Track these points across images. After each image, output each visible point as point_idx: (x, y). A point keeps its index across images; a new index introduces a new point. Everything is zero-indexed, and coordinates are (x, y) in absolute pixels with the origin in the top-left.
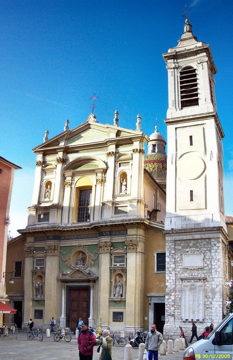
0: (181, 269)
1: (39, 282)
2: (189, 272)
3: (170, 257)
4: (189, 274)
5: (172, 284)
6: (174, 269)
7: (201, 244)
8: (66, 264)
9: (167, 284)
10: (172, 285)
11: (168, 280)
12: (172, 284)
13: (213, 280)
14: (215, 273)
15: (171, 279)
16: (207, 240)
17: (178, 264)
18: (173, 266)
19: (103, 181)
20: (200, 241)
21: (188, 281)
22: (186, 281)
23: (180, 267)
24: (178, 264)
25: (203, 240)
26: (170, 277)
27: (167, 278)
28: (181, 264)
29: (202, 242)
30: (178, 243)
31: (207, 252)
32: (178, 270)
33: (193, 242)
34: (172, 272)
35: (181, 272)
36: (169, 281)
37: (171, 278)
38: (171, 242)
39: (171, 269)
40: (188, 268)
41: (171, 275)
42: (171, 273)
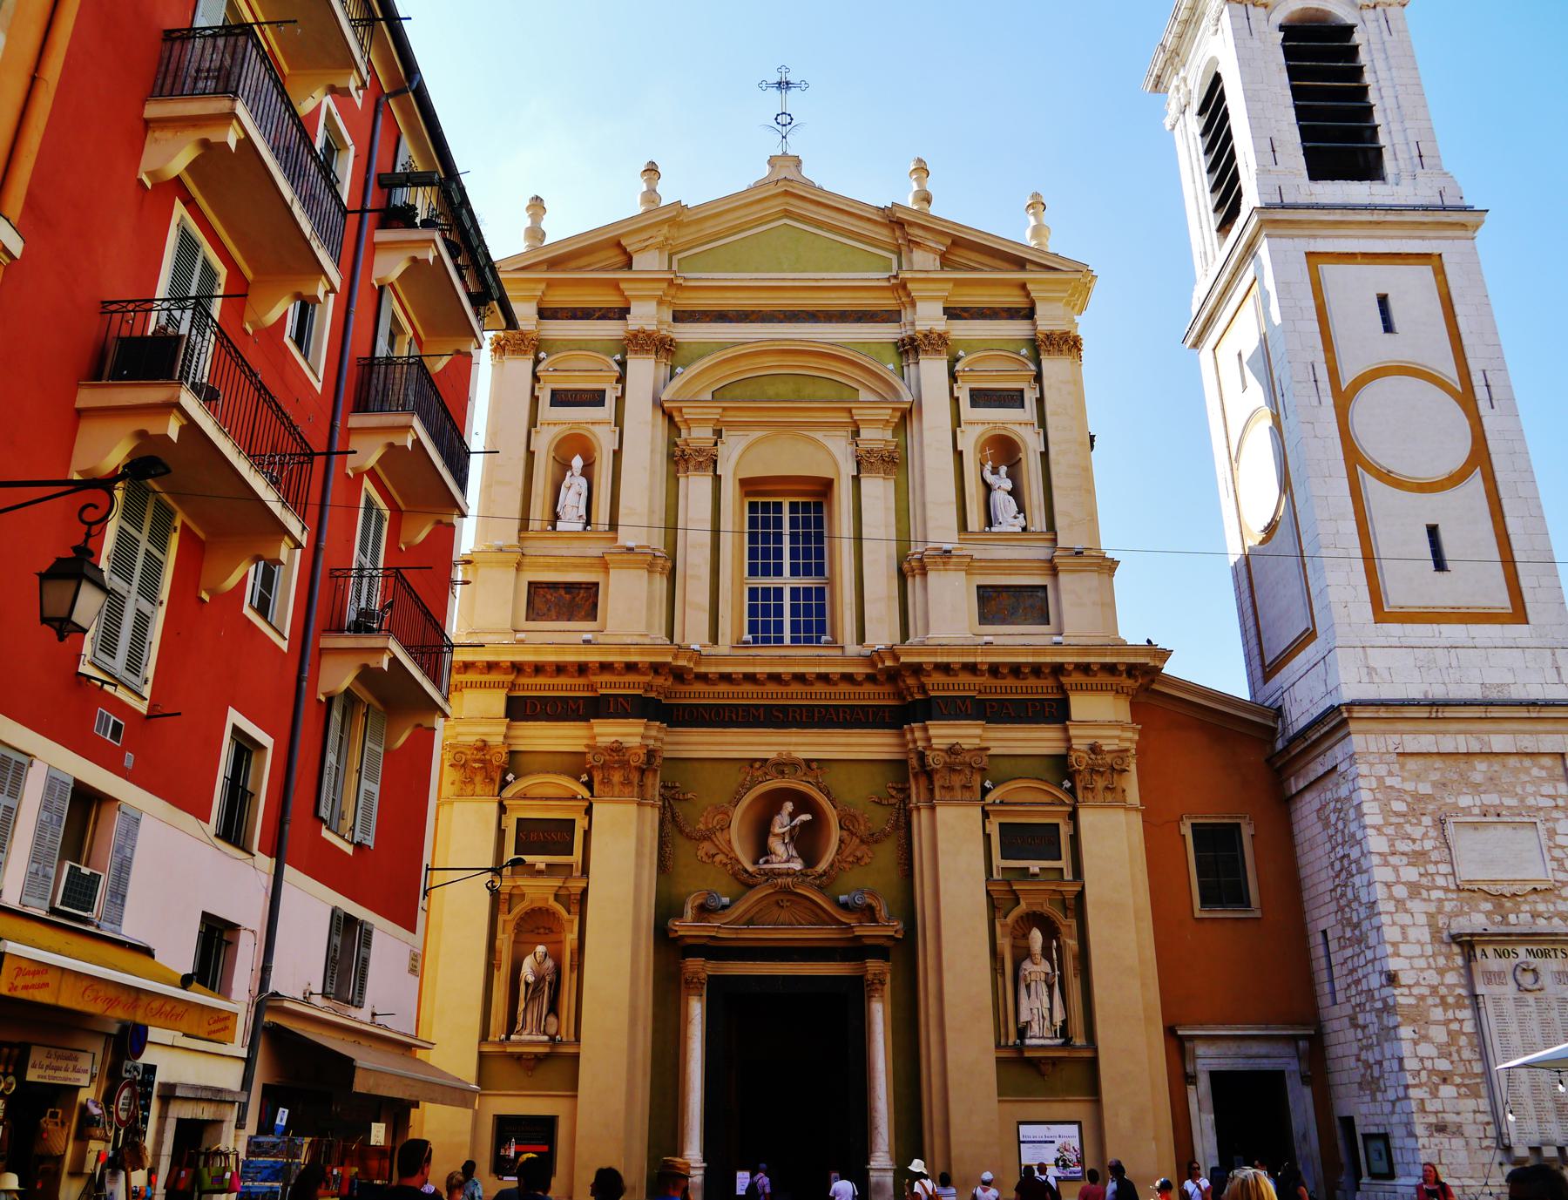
0: (1446, 890)
1: (541, 949)
2: (1488, 906)
4: (1488, 914)
6: (1414, 889)
7: (1525, 778)
8: (701, 853)
9: (1393, 964)
10: (1422, 970)
11: (1394, 944)
12: (1422, 963)
16: (1547, 761)
17: (1431, 869)
18: (1411, 874)
19: (893, 462)
20: (1512, 762)
21: (1500, 948)
22: (1489, 950)
23: (1440, 881)
24: (1431, 869)
25: (1527, 762)
26: (1403, 927)
27: (1392, 934)
28: (1445, 868)
29: (1527, 771)
31: (1555, 814)
32: (1436, 894)
33: (1481, 766)
34: (1409, 904)
35: (1448, 906)
36: (1403, 949)
37: (1413, 934)
39: (1400, 891)
40: (1485, 888)
41: (1404, 919)
42: (1406, 911)
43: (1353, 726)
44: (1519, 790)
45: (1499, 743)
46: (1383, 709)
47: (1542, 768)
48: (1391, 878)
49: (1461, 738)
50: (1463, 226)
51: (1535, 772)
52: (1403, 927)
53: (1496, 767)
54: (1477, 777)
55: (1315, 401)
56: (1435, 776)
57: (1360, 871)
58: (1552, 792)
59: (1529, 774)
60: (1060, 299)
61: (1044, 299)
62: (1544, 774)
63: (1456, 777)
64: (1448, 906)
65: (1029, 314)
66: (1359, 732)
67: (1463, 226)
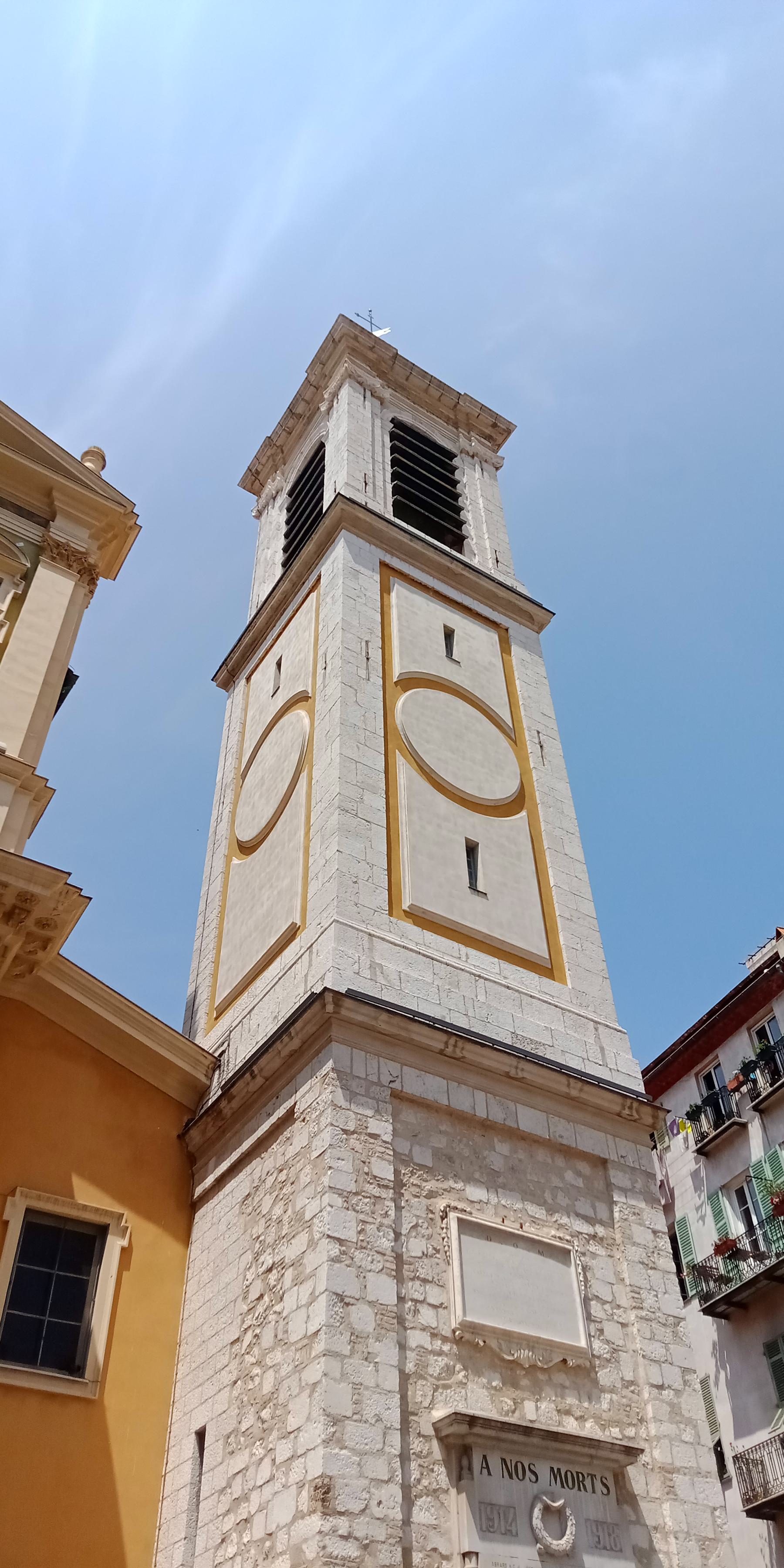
3: (364, 1204)
5: (379, 1468)
7: (556, 1182)
13: (671, 1490)
14: (668, 1428)
15: (369, 1413)
18: (384, 1290)
20: (542, 1155)
25: (560, 1161)
26: (357, 1387)
28: (434, 1295)
30: (410, 1116)
31: (593, 1247)
33: (503, 1148)
34: (375, 1347)
37: (373, 1405)
38: (367, 1095)
43: (335, 1031)
44: (548, 1196)
45: (530, 1120)
46: (384, 1016)
47: (579, 1174)
48: (352, 1290)
49: (480, 1096)
50: (531, 618)
51: (569, 1175)
52: (357, 1387)
53: (521, 1155)
54: (498, 1163)
55: (363, 673)
56: (440, 1142)
57: (298, 1282)
58: (590, 1213)
59: (562, 1178)
60: (89, 526)
61: (68, 516)
62: (580, 1183)
63: (466, 1152)
64: (436, 1365)
65: (45, 523)
66: (343, 1042)
67: (531, 618)
